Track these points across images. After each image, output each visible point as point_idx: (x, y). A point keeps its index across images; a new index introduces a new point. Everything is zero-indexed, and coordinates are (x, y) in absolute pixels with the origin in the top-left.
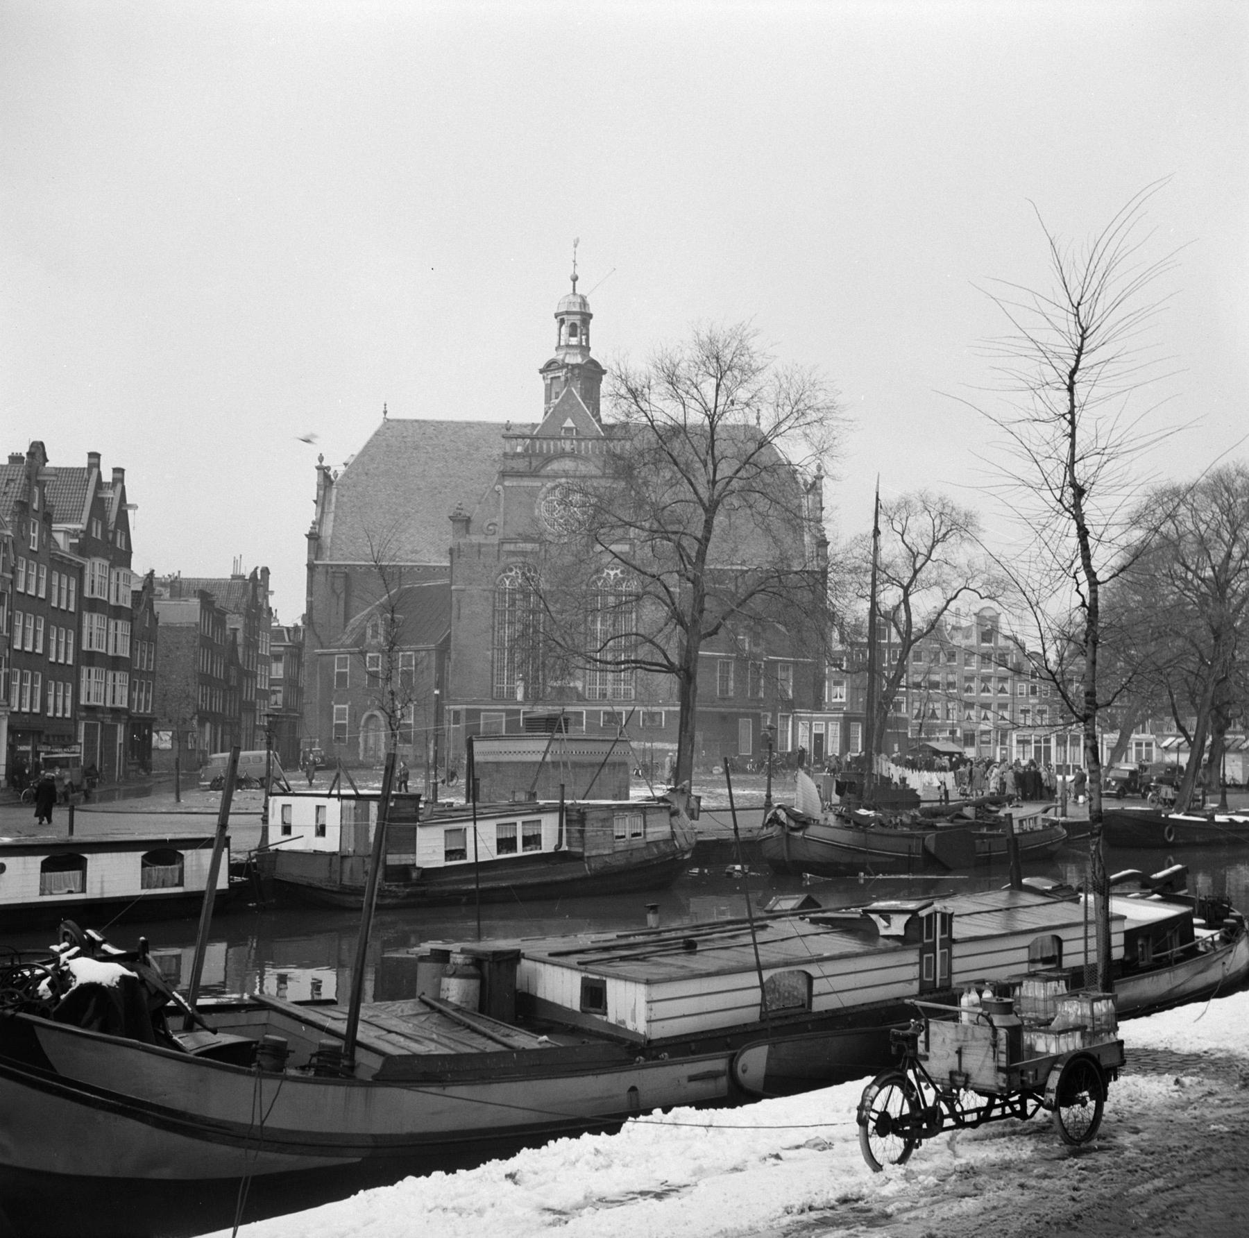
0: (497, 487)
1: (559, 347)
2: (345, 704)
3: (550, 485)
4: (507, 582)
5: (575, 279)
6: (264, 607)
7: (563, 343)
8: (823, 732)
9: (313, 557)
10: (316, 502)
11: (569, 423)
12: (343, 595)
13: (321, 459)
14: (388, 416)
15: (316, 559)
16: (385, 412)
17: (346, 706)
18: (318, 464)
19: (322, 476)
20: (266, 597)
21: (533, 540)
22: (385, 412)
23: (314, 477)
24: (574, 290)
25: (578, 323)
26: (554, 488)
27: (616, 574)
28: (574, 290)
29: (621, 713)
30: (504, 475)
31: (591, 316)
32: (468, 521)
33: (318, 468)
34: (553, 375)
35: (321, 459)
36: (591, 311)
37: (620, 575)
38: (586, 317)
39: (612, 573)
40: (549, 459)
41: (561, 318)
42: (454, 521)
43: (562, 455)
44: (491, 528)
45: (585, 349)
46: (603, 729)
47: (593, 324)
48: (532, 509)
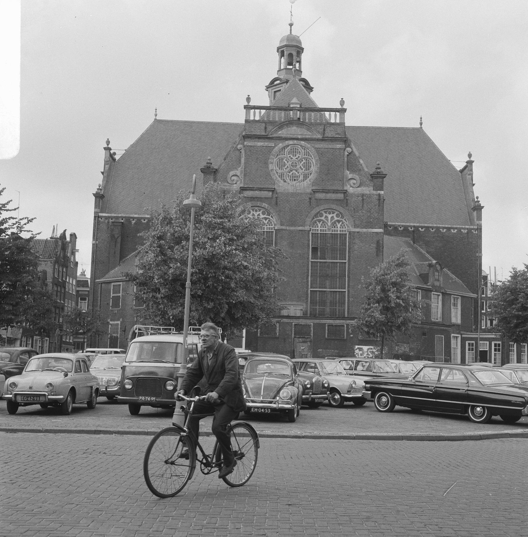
0: (239, 147)
1: (280, 70)
2: (118, 320)
3: (281, 145)
5: (291, 25)
6: (72, 260)
7: (282, 67)
8: (488, 349)
10: (103, 173)
12: (119, 240)
13: (108, 142)
14: (158, 118)
15: (101, 212)
16: (156, 115)
17: (119, 322)
18: (106, 146)
19: (108, 155)
20: (73, 253)
21: (268, 190)
22: (156, 115)
23: (102, 155)
24: (291, 32)
26: (284, 148)
27: (332, 217)
28: (291, 32)
29: (343, 326)
30: (246, 137)
32: (215, 172)
33: (105, 148)
34: (275, 90)
35: (108, 142)
36: (303, 46)
37: (336, 219)
38: (300, 50)
39: (330, 216)
44: (233, 178)
45: (300, 71)
46: (326, 339)
47: (304, 56)
48: (266, 163)
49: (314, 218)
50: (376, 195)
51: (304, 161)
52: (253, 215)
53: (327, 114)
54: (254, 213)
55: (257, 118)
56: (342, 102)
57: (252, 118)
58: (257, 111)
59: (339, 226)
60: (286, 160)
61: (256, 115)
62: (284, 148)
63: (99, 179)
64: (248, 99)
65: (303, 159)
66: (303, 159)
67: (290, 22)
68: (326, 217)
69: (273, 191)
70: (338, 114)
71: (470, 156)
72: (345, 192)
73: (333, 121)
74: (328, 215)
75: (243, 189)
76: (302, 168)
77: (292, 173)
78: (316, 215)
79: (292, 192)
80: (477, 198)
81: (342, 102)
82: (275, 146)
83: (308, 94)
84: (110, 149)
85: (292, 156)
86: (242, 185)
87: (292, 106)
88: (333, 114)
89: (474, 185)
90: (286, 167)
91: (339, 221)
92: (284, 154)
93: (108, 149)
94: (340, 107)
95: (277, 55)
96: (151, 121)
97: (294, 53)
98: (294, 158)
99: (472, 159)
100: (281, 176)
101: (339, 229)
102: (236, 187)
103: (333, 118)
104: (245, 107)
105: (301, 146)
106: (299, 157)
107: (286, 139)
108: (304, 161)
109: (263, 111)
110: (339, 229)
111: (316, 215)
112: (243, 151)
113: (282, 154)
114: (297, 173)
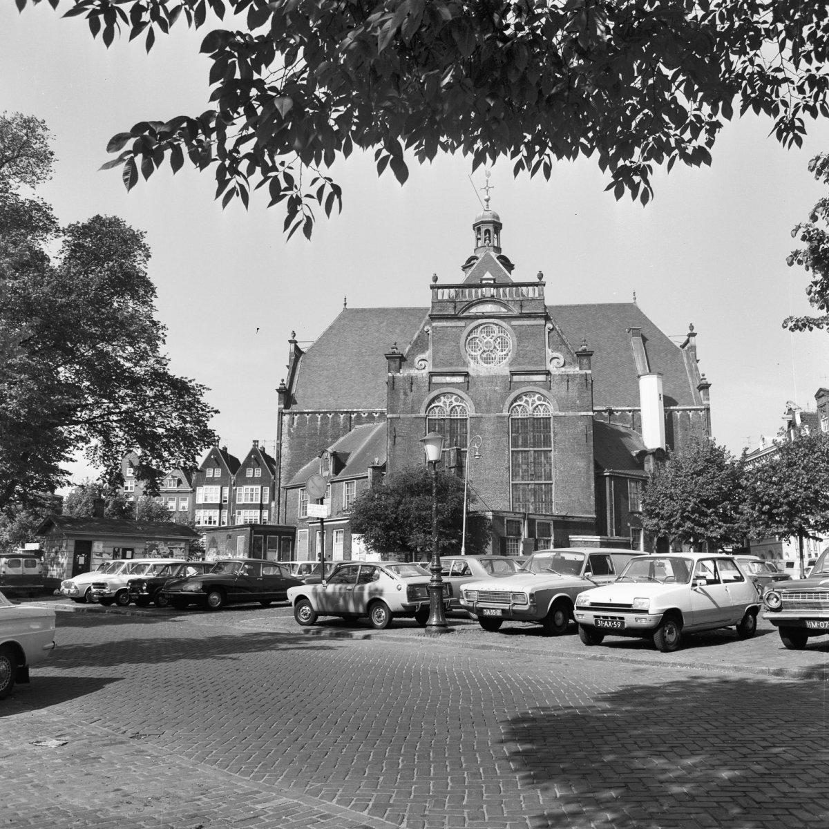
4: (437, 411)
9: (282, 406)
11: (488, 275)
14: (347, 307)
16: (345, 304)
18: (291, 339)
22: (345, 304)
30: (433, 318)
31: (501, 225)
36: (501, 221)
38: (498, 227)
40: (471, 305)
41: (477, 227)
42: (387, 358)
43: (483, 301)
47: (502, 232)
49: (512, 404)
50: (582, 375)
52: (445, 402)
53: (524, 289)
54: (446, 400)
55: (446, 297)
56: (541, 276)
57: (440, 297)
58: (446, 291)
59: (542, 410)
61: (445, 294)
62: (477, 327)
63: (285, 374)
64: (435, 279)
67: (487, 197)
68: (526, 401)
69: (467, 375)
70: (536, 288)
71: (692, 327)
72: (548, 373)
73: (531, 295)
74: (528, 399)
75: (432, 374)
78: (515, 400)
79: (488, 374)
80: (703, 375)
81: (541, 276)
83: (508, 274)
84: (296, 342)
86: (431, 370)
87: (484, 282)
88: (531, 288)
89: (698, 361)
91: (541, 405)
93: (293, 342)
94: (537, 280)
95: (473, 234)
96: (341, 309)
97: (492, 230)
99: (694, 331)
100: (474, 358)
101: (542, 414)
102: (425, 373)
103: (531, 292)
104: (432, 287)
105: (496, 325)
107: (477, 318)
108: (499, 340)
109: (452, 291)
110: (541, 414)
111: (515, 400)
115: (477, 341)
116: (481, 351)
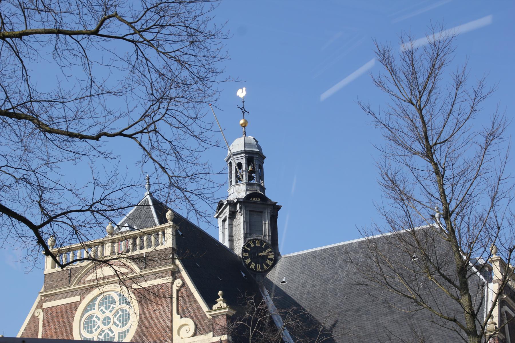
25: (243, 162)
26: (94, 299)
51: (120, 313)
60: (97, 317)
65: (119, 311)
66: (119, 311)
76: (118, 323)
77: (103, 334)
82: (82, 299)
85: (104, 310)
90: (96, 327)
92: (94, 309)
98: (107, 312)
106: (113, 308)
112: (41, 317)
113: (91, 310)
114: (110, 333)
115: (94, 319)
116: (99, 330)
